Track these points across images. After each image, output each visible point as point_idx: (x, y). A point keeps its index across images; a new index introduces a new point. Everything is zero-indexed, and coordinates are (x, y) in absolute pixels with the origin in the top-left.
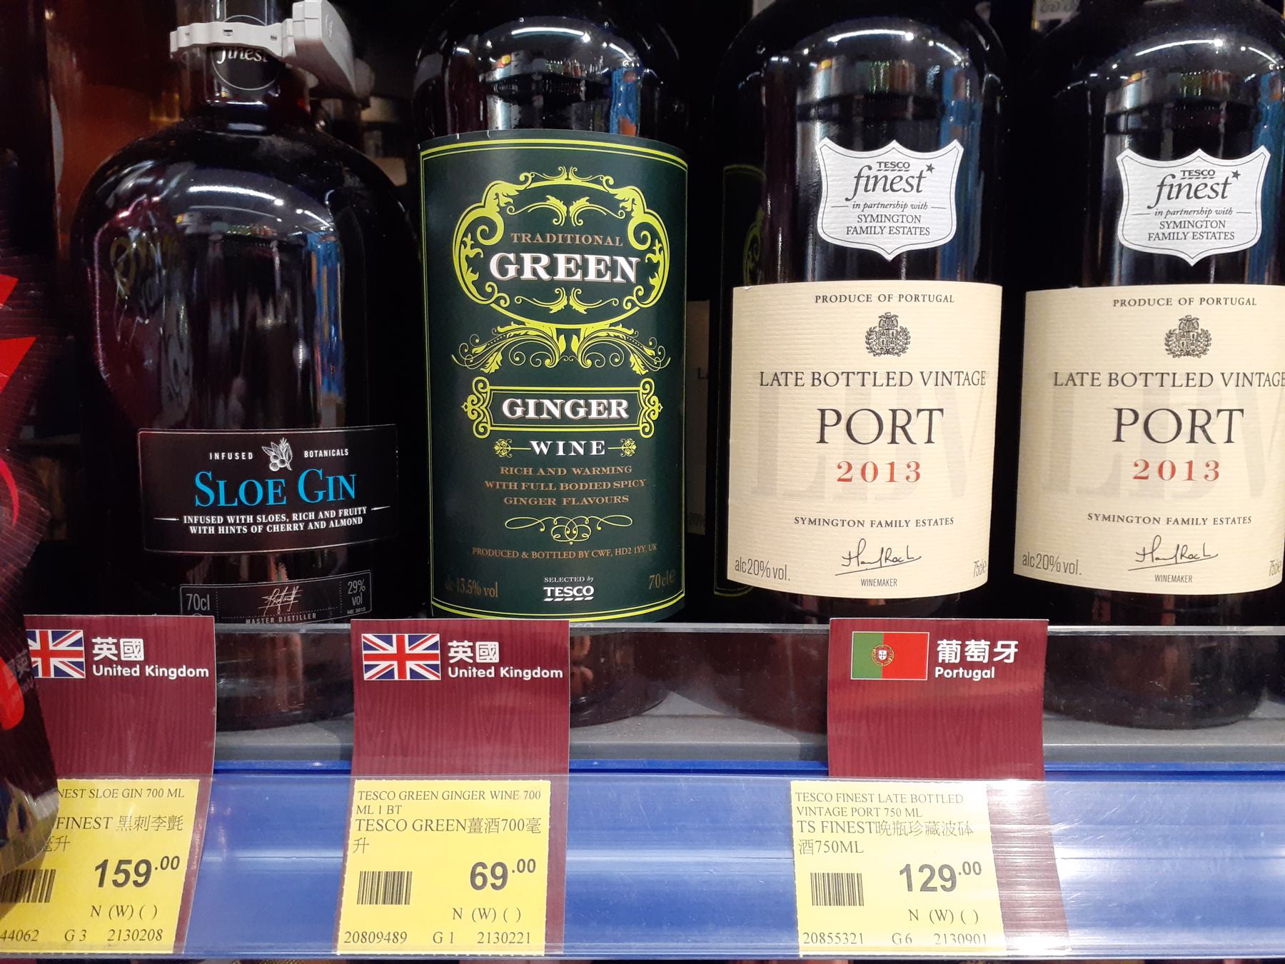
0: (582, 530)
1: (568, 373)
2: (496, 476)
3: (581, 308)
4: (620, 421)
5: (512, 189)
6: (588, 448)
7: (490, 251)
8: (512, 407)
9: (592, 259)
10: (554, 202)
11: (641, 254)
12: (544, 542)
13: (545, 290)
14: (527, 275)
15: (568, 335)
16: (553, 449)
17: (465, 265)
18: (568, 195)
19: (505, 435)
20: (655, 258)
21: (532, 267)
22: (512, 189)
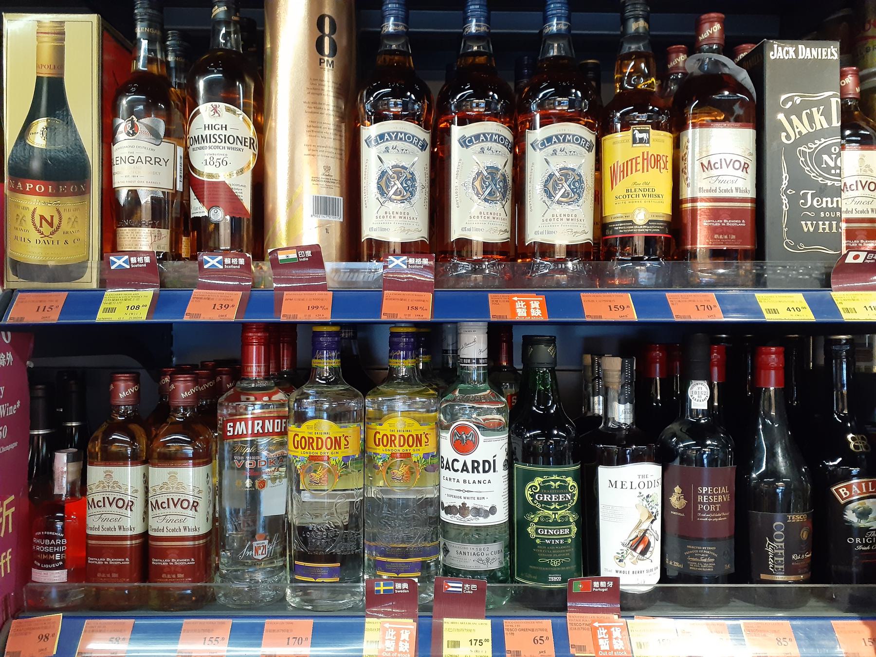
0: (558, 563)
1: (555, 523)
2: (536, 548)
3: (558, 507)
4: (568, 534)
5: (542, 480)
6: (560, 542)
7: (536, 493)
8: (541, 531)
9: (561, 495)
10: (552, 483)
11: (571, 493)
12: (548, 565)
13: (549, 503)
14: (545, 500)
15: (555, 514)
16: (551, 542)
17: (529, 495)
18: (555, 481)
19: (539, 538)
20: (574, 492)
21: (546, 498)
22: (542, 480)
